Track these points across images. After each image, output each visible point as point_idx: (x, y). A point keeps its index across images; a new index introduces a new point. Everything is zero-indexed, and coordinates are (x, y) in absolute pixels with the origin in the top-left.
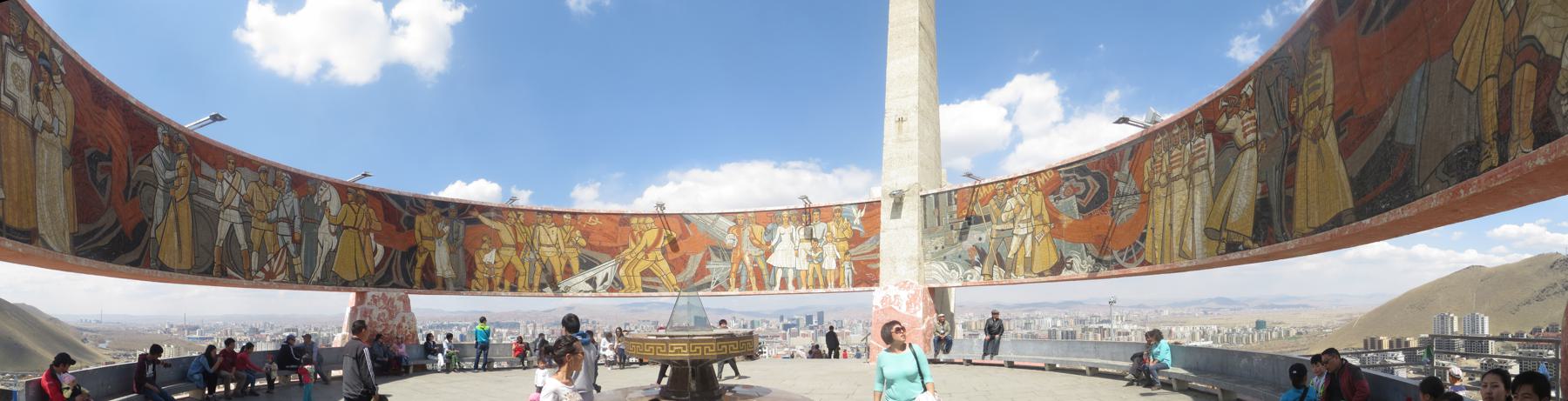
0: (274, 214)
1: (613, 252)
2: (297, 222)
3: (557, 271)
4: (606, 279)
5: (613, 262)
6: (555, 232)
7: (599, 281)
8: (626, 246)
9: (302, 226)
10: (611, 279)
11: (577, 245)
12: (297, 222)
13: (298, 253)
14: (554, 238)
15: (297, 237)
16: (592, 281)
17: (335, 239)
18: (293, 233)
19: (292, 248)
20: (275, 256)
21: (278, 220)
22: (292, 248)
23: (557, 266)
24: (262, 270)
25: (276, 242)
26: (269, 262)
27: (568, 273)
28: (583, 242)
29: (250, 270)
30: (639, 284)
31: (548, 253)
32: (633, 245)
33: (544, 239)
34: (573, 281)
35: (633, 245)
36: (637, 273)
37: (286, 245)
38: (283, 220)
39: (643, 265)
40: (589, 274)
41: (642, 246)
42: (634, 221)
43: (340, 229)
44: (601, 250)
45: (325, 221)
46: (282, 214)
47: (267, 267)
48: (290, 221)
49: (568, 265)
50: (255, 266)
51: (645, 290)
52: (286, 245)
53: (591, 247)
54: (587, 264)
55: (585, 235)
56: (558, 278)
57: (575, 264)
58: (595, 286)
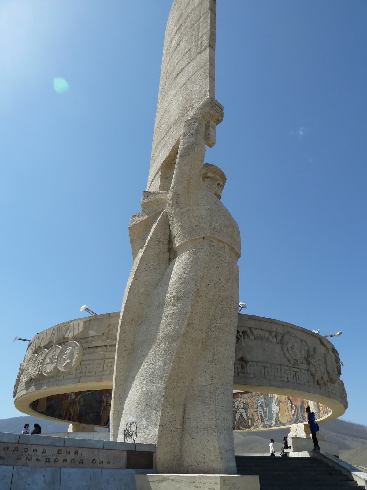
2: (264, 406)
9: (266, 407)
12: (264, 406)
13: (266, 416)
15: (265, 411)
17: (278, 407)
18: (263, 411)
19: (263, 415)
21: (257, 407)
22: (263, 415)
25: (257, 415)
29: (249, 426)
37: (261, 415)
38: (259, 406)
43: (279, 403)
45: (274, 402)
46: (259, 404)
47: (255, 424)
48: (262, 406)
50: (250, 424)
52: (261, 415)
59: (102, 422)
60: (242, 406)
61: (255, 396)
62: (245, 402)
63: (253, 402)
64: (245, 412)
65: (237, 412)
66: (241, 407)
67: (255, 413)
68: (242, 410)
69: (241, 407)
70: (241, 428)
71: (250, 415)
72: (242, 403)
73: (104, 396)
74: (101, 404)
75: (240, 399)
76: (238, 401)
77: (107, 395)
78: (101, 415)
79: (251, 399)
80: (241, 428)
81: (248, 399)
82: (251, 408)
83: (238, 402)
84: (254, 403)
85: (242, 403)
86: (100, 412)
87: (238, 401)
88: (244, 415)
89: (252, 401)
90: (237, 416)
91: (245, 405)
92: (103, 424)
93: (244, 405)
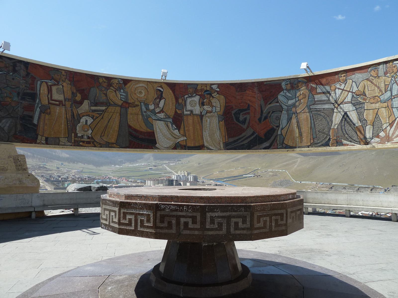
0: (389, 94)
20: (391, 125)
24: (378, 136)
26: (384, 130)
29: (365, 138)
47: (382, 134)
50: (369, 134)
59: (39, 137)
60: (349, 98)
61: (385, 73)
62: (355, 89)
63: (378, 88)
64: (356, 109)
65: (335, 110)
66: (346, 100)
67: (384, 113)
68: (348, 108)
69: (346, 100)
70: (345, 142)
71: (369, 116)
72: (349, 92)
73: (39, 83)
74: (34, 100)
75: (343, 85)
76: (339, 89)
77: (46, 83)
78: (35, 122)
79: (374, 81)
80: (345, 142)
81: (366, 82)
82: (372, 101)
83: (338, 92)
84: (381, 91)
85: (349, 92)
86: (32, 117)
87: (339, 89)
88: (354, 116)
89: (376, 85)
90: (334, 119)
91: (357, 95)
92: (44, 142)
93: (353, 96)
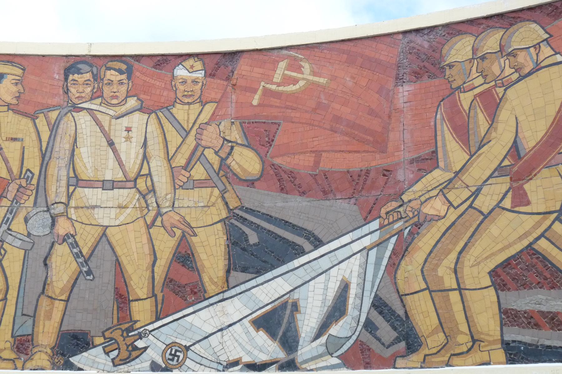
1: (369, 191)
3: (139, 285)
4: (337, 310)
5: (368, 235)
6: (135, 130)
7: (308, 321)
8: (428, 161)
10: (359, 307)
11: (225, 173)
14: (131, 154)
16: (276, 321)
23: (141, 258)
27: (182, 288)
28: (247, 162)
30: (488, 322)
31: (108, 210)
32: (454, 152)
33: (92, 158)
34: (201, 320)
35: (454, 152)
36: (477, 274)
39: (506, 235)
40: (269, 289)
41: (496, 152)
42: (460, 50)
44: (323, 186)
49: (185, 257)
51: (516, 354)
53: (283, 180)
54: (259, 249)
55: (260, 135)
56: (141, 311)
57: (212, 253)
58: (289, 342)
